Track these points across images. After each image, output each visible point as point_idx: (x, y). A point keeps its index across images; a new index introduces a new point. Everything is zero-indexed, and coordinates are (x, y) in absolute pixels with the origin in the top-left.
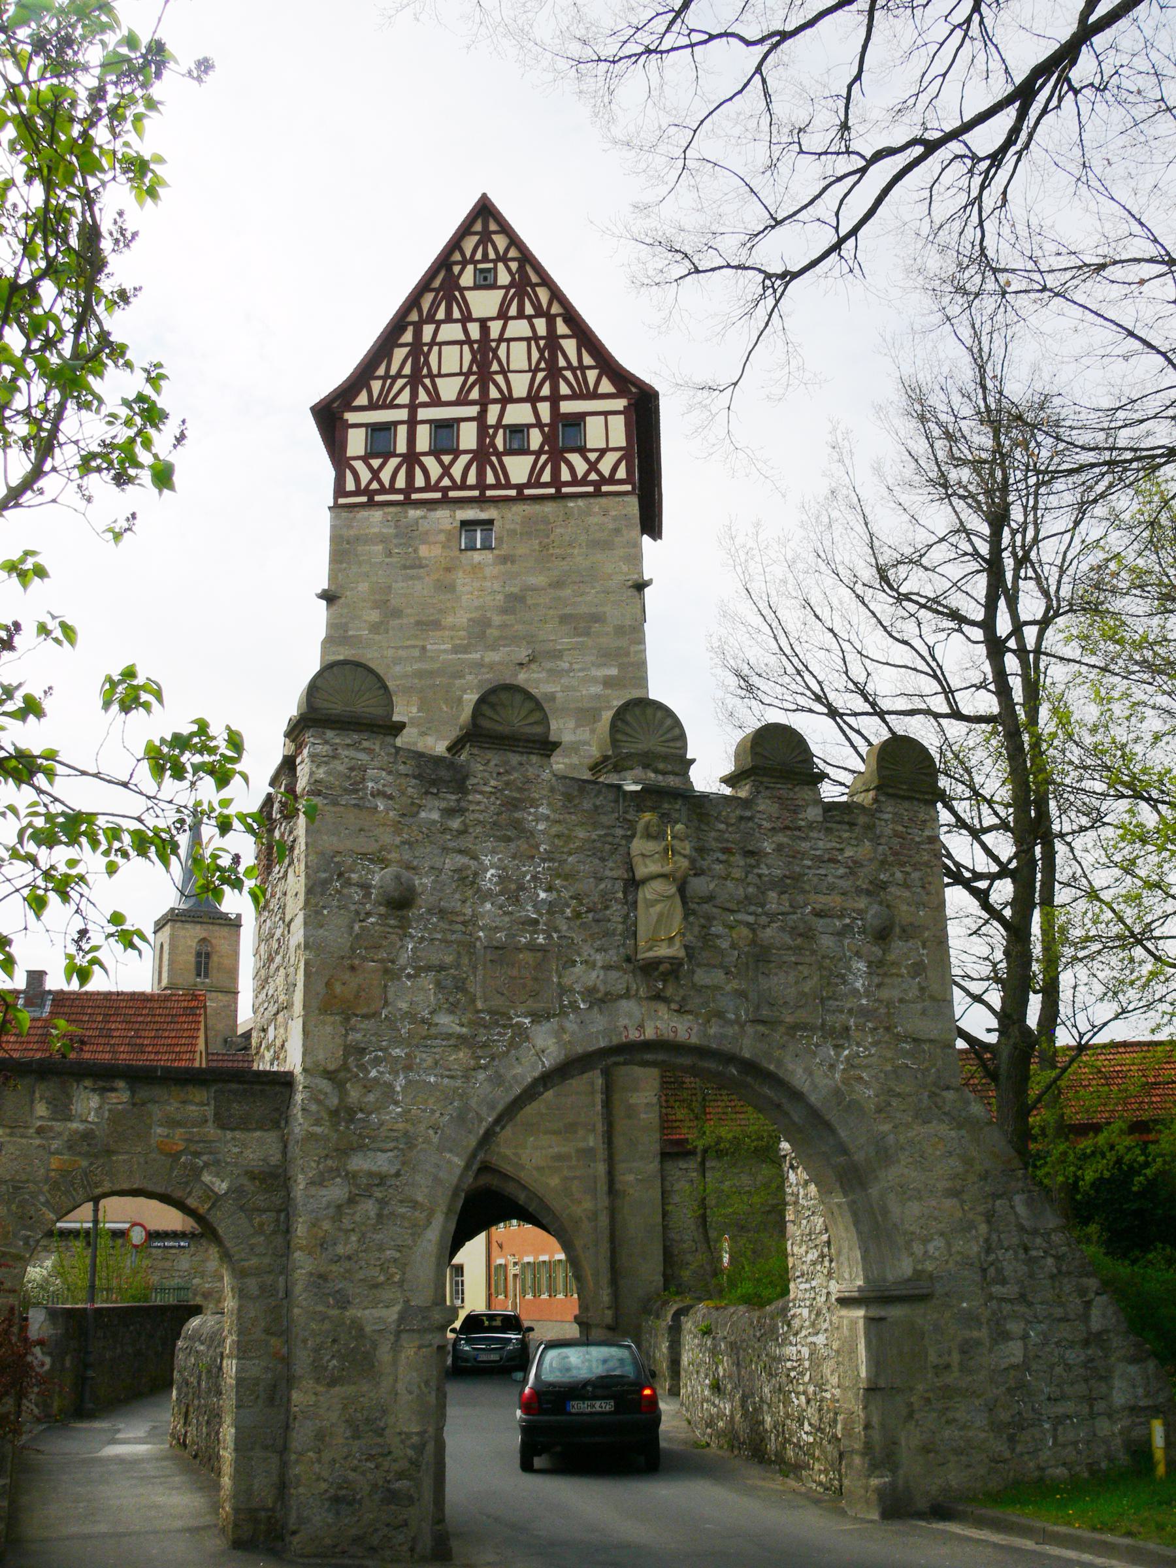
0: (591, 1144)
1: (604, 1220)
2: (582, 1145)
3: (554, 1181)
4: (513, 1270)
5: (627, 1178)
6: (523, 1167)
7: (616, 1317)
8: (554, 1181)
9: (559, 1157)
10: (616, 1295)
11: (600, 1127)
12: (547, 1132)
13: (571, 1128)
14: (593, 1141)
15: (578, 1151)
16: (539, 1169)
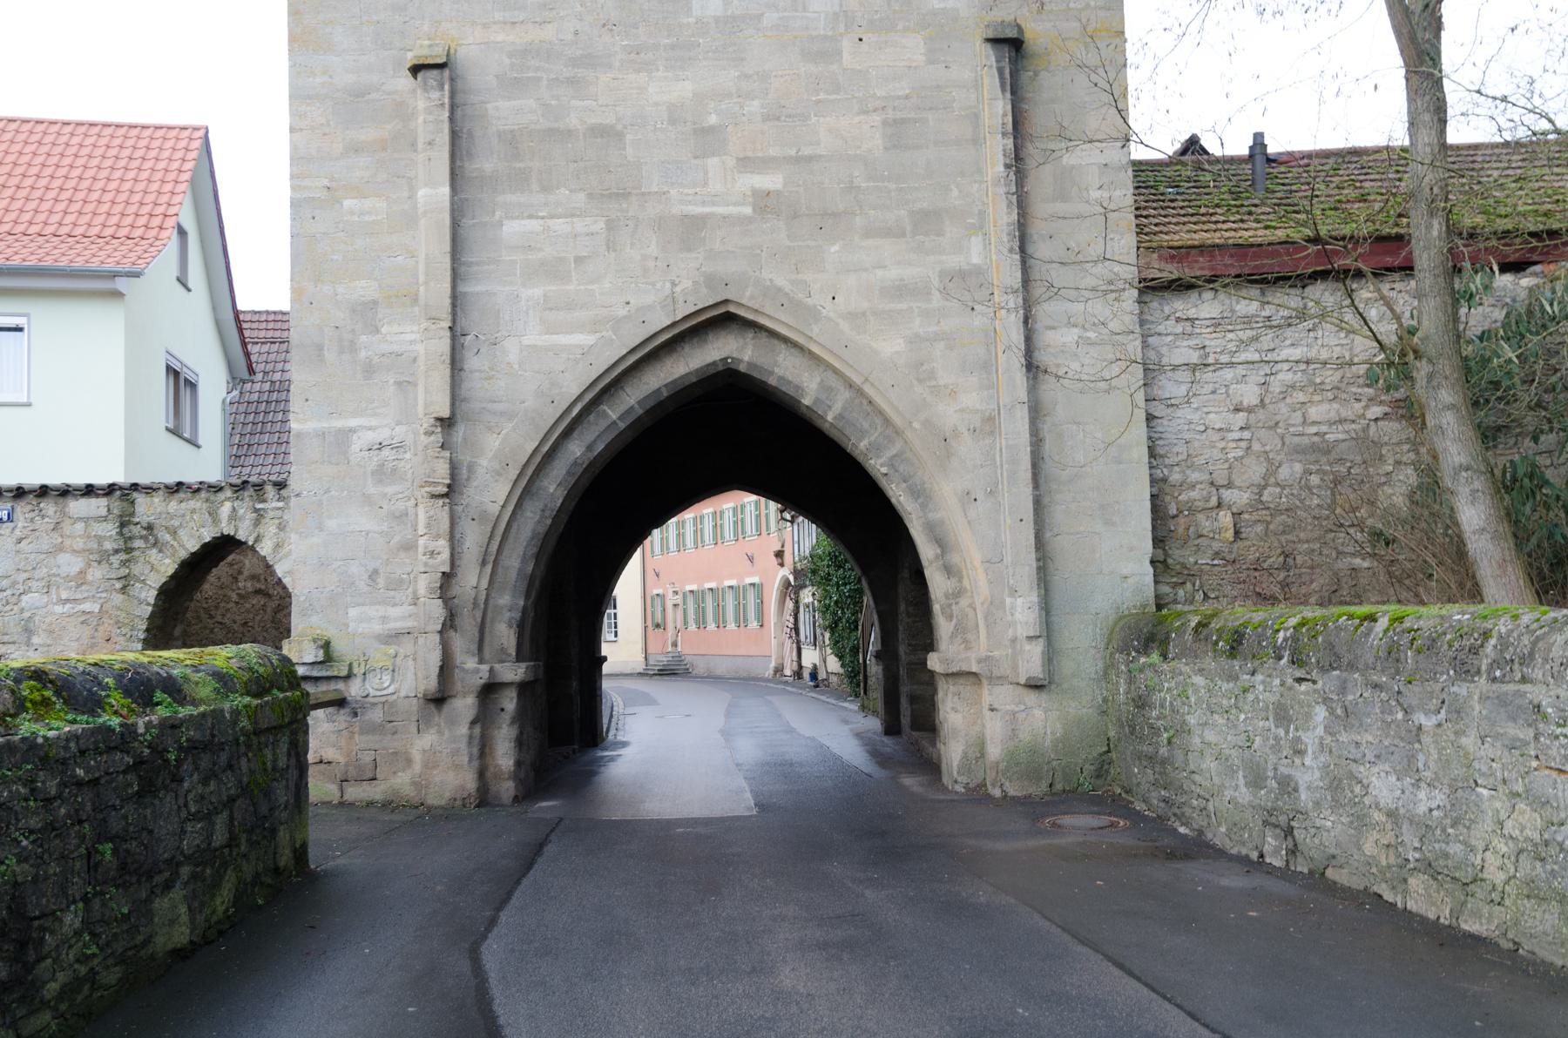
0: (976, 259)
1: (1017, 426)
2: (953, 261)
3: (891, 346)
4: (671, 600)
5: (1057, 340)
6: (814, 314)
7: (1050, 657)
8: (891, 346)
9: (900, 290)
10: (1046, 607)
11: (1003, 217)
12: (868, 233)
13: (927, 221)
14: (987, 251)
15: (942, 274)
16: (855, 317)
